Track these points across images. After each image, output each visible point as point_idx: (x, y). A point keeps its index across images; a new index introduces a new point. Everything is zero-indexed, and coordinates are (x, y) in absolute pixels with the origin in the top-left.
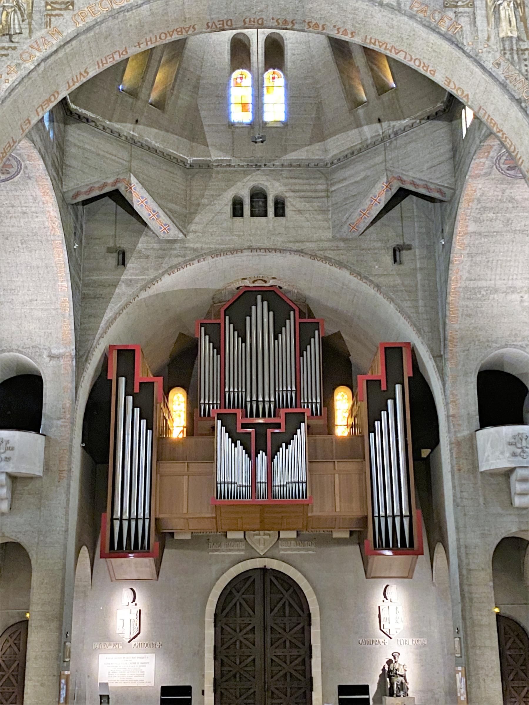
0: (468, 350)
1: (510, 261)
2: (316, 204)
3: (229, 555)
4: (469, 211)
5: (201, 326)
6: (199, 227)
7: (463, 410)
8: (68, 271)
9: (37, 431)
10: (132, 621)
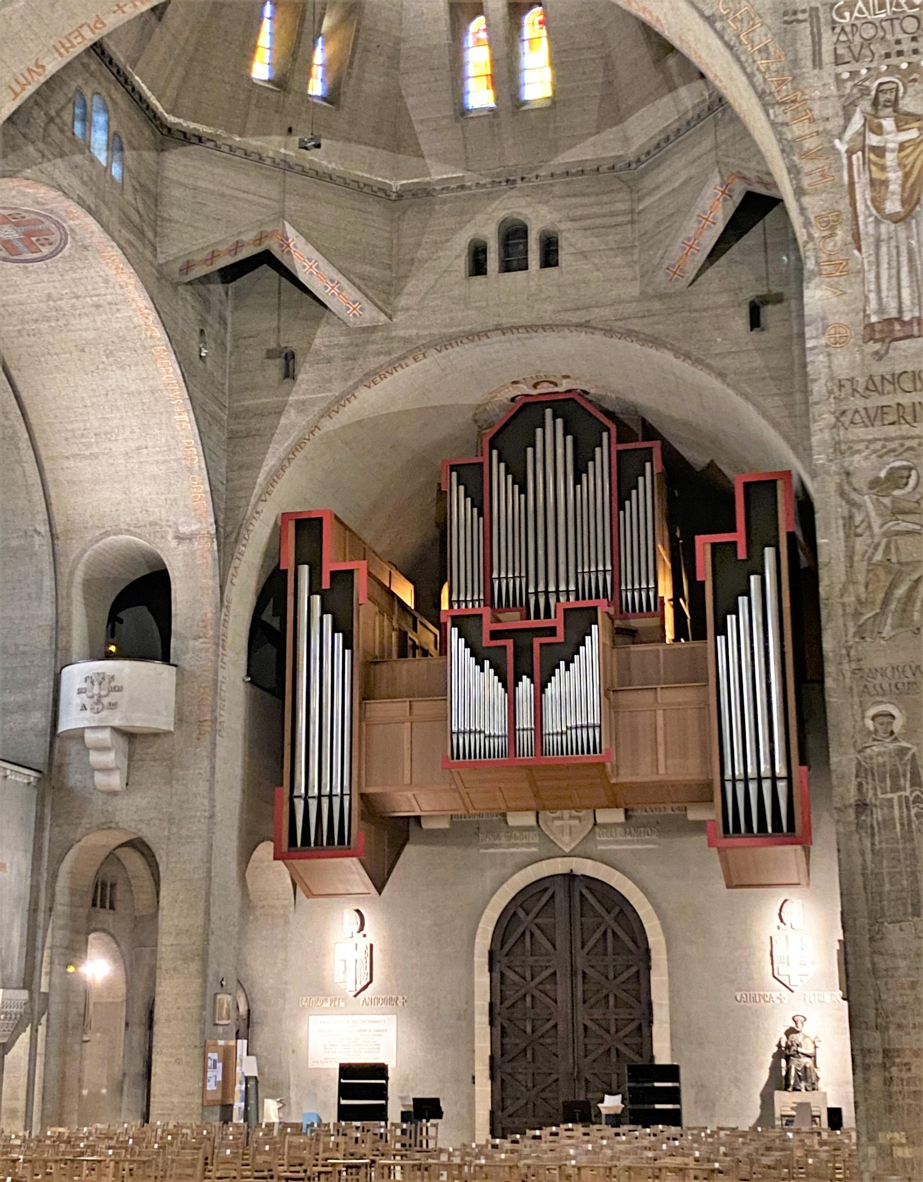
2: (612, 238)
3: (512, 854)
5: (451, 471)
8: (186, 396)
9: (165, 658)
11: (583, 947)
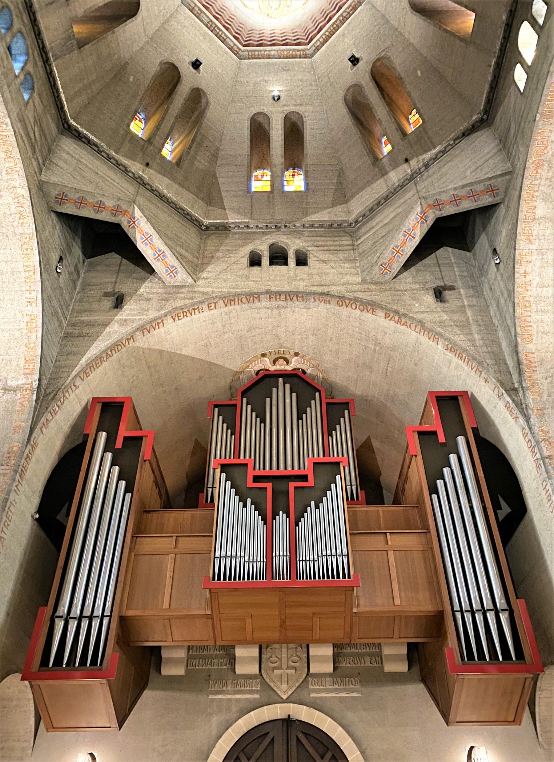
2: (341, 256)
4: (537, 182)
5: (214, 408)
6: (209, 275)
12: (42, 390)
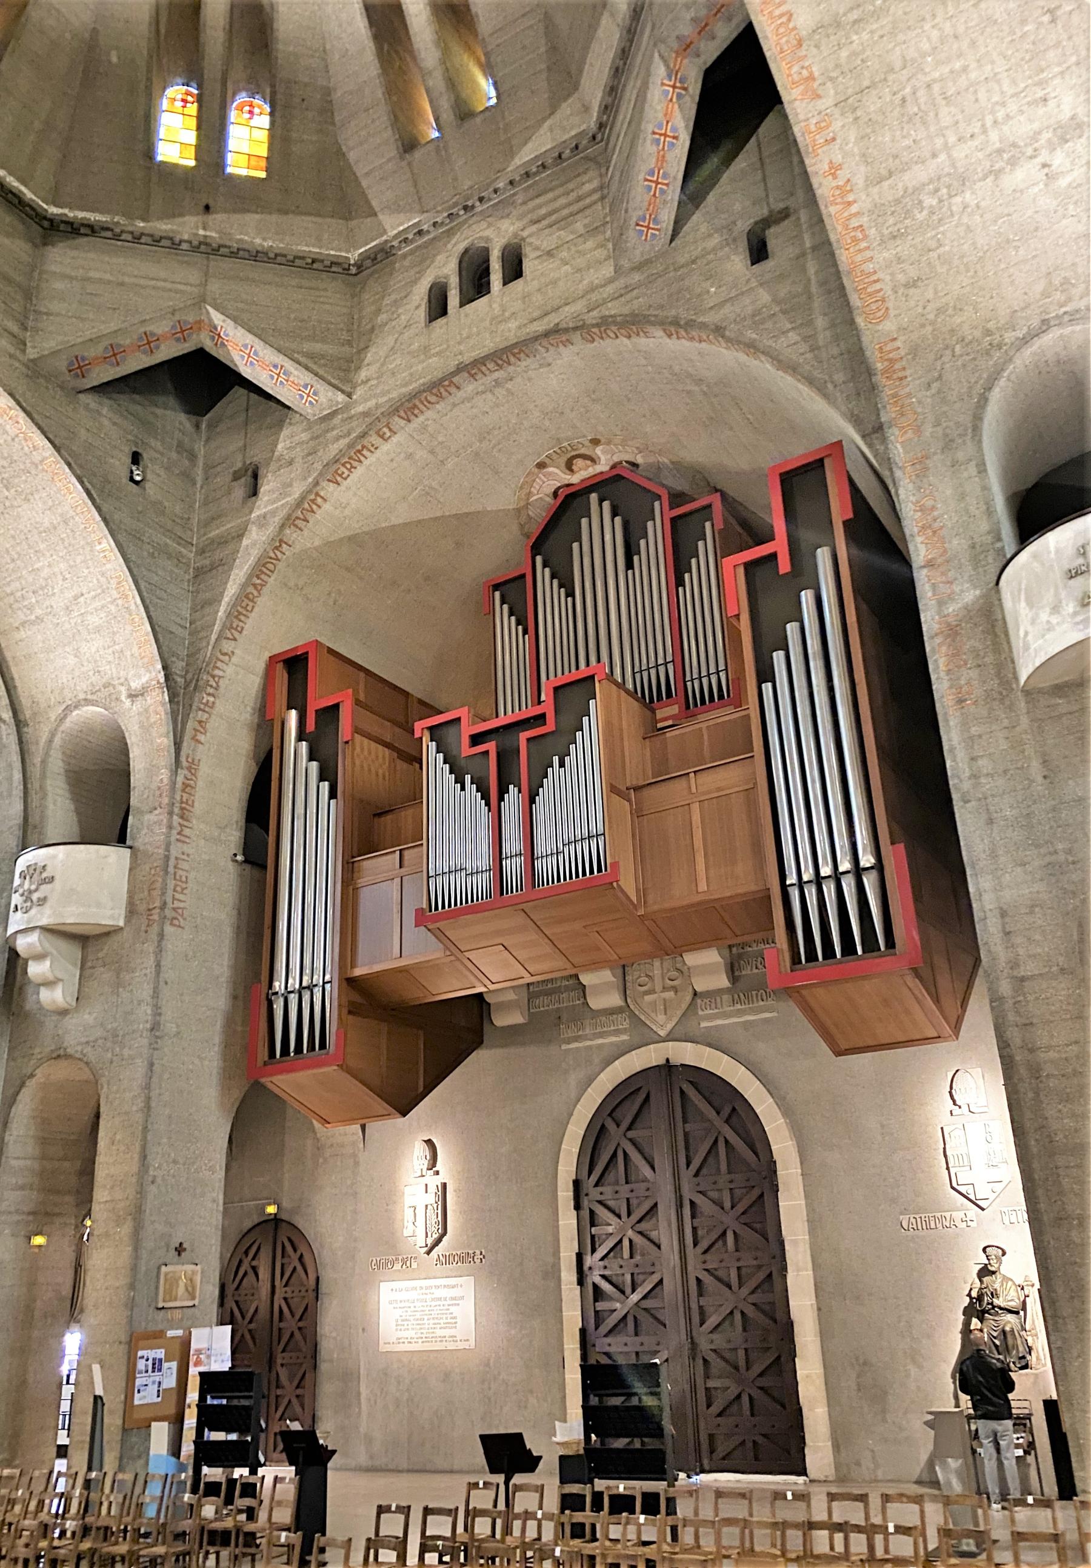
0: (940, 377)
1: (965, 69)
7: (955, 542)
9: (121, 839)
10: (429, 1207)
11: (688, 1165)
12: (179, 679)
